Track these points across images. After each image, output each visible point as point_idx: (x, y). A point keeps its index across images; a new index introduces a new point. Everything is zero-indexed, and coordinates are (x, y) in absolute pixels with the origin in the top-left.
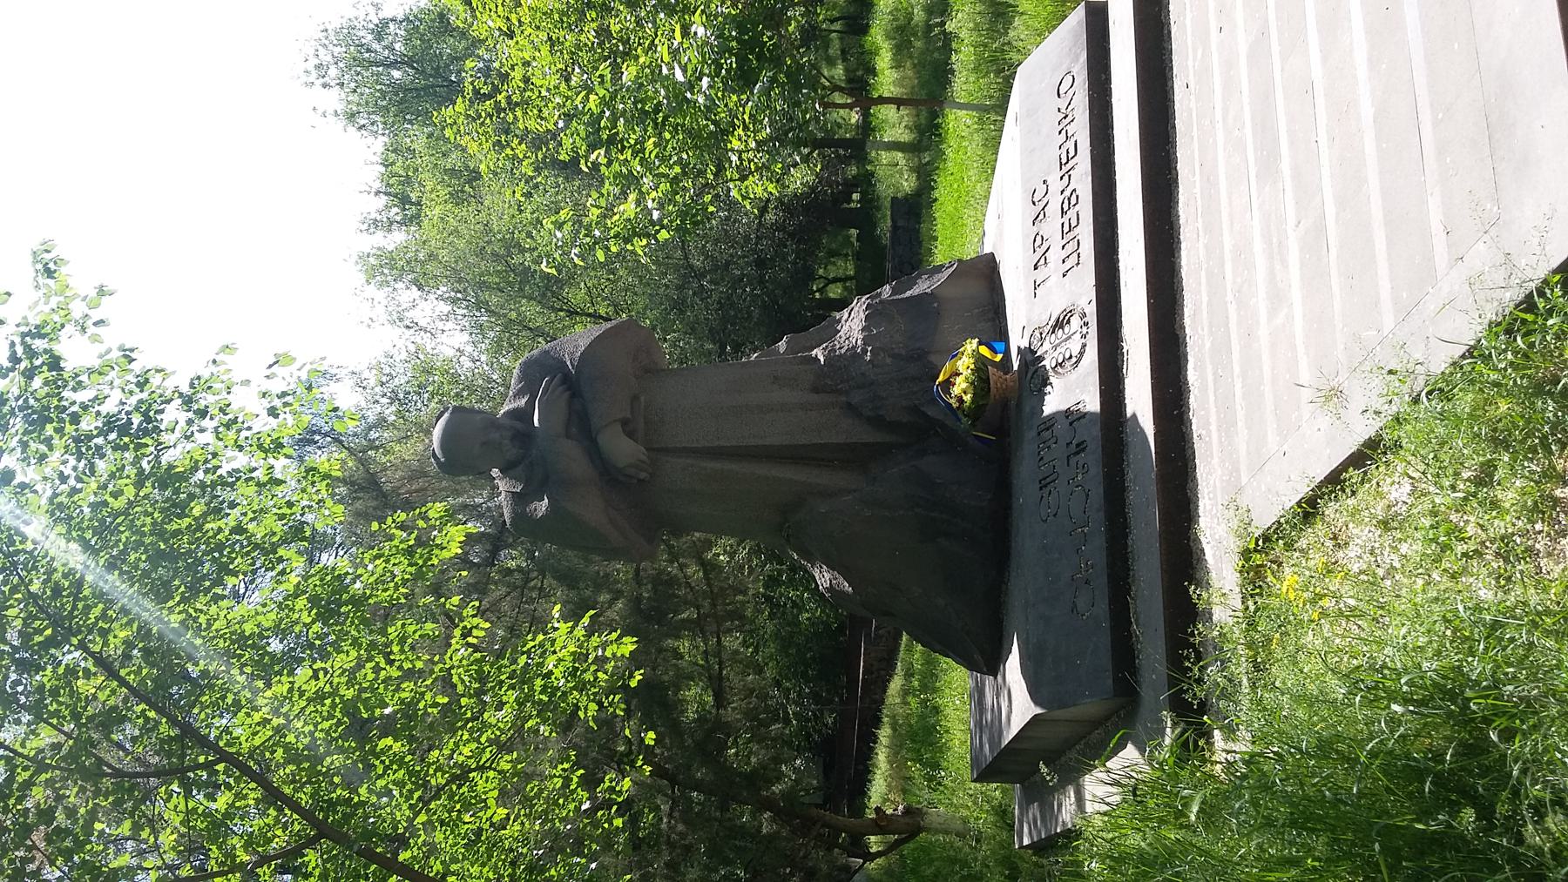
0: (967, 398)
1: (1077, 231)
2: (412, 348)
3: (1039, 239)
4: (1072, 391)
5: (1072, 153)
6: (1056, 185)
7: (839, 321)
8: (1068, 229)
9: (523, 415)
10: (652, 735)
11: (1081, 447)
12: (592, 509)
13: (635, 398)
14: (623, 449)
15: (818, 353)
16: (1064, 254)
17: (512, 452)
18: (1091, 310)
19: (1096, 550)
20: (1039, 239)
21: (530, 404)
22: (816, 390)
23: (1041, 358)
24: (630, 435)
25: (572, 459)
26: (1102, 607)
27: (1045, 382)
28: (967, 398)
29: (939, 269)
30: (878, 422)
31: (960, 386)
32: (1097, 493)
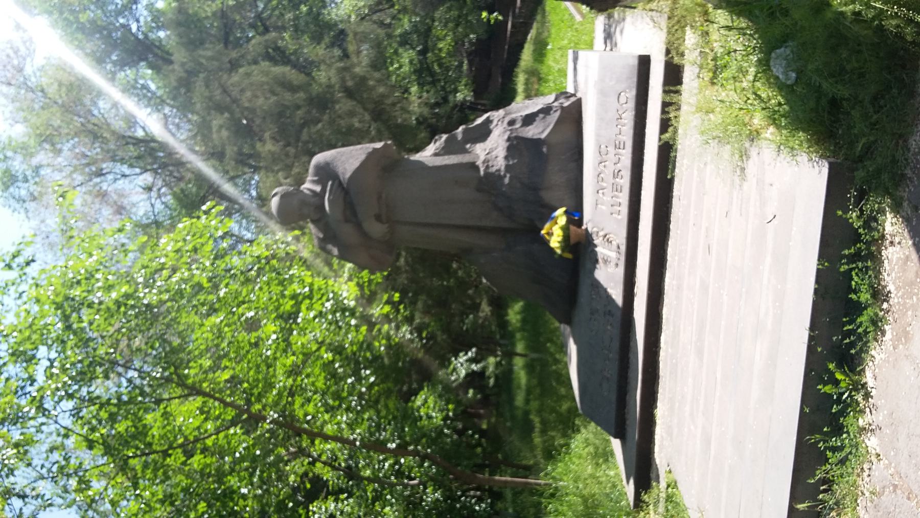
0: (559, 251)
1: (621, 194)
3: (600, 179)
4: (609, 276)
5: (622, 147)
7: (491, 122)
8: (617, 189)
10: (397, 295)
11: (610, 313)
14: (377, 229)
18: (623, 248)
19: (612, 370)
20: (600, 179)
23: (596, 246)
24: (378, 218)
25: (348, 232)
26: (613, 397)
27: (597, 261)
28: (559, 251)
29: (546, 110)
31: (555, 242)
32: (616, 345)
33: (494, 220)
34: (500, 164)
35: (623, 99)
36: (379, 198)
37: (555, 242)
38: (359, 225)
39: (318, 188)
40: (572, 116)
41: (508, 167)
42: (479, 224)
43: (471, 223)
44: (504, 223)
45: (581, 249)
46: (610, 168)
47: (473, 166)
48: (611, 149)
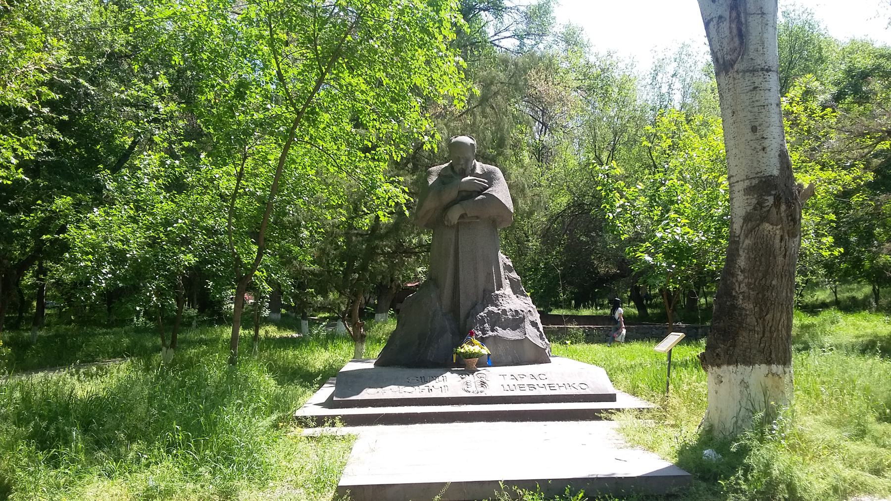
2: (632, 77)
6: (541, 383)
8: (521, 387)
9: (473, 172)
12: (431, 204)
13: (477, 217)
14: (454, 215)
15: (507, 290)
16: (511, 386)
17: (457, 169)
18: (483, 395)
21: (478, 175)
22: (484, 291)
24: (462, 217)
25: (451, 194)
28: (462, 350)
30: (468, 316)
31: (467, 348)
33: (465, 305)
34: (507, 307)
35: (583, 386)
36: (477, 217)
37: (467, 348)
38: (454, 202)
39: (478, 171)
40: (541, 357)
41: (504, 311)
42: (461, 292)
43: (461, 286)
44: (463, 312)
45: (465, 365)
46: (534, 382)
47: (500, 286)
48: (546, 382)
